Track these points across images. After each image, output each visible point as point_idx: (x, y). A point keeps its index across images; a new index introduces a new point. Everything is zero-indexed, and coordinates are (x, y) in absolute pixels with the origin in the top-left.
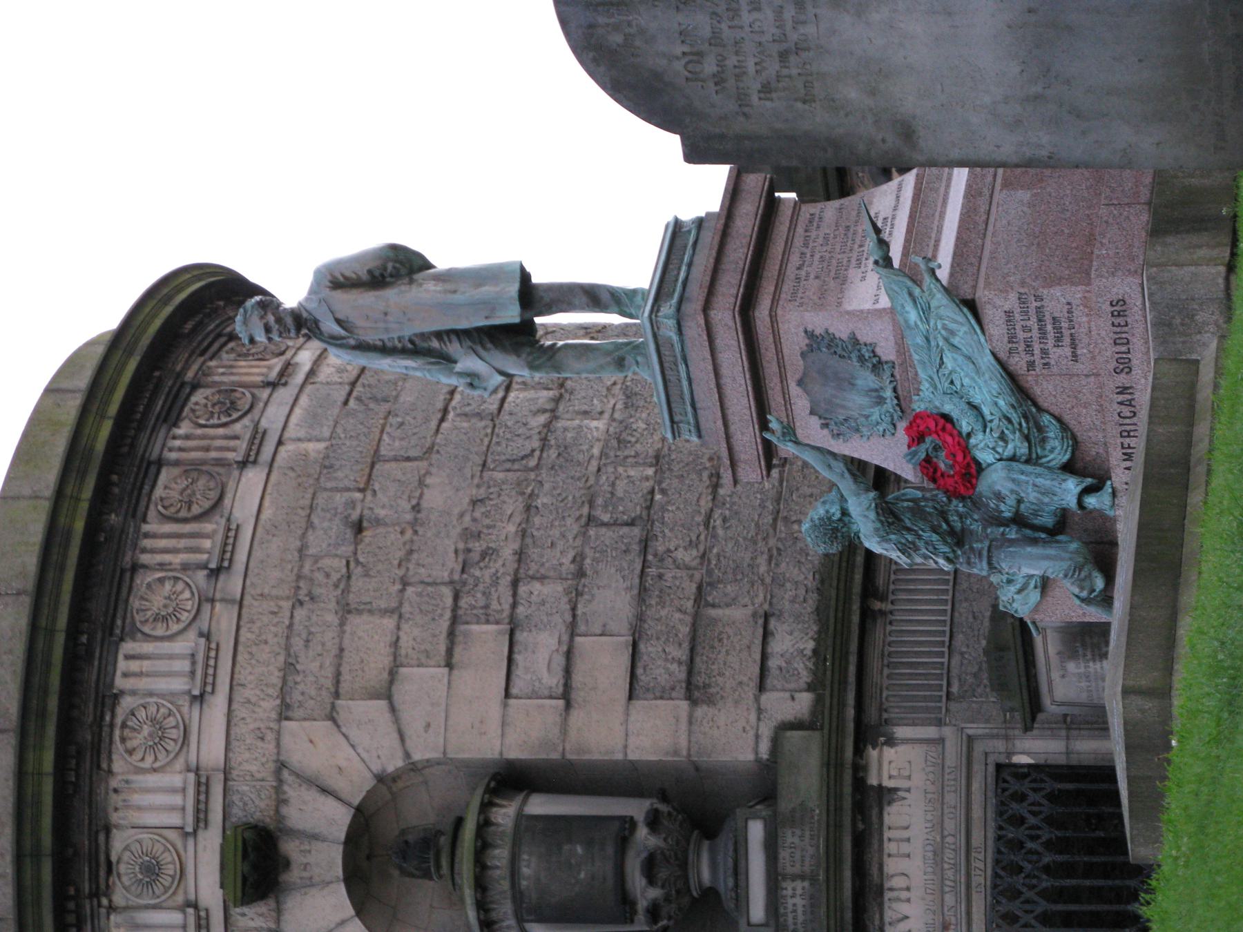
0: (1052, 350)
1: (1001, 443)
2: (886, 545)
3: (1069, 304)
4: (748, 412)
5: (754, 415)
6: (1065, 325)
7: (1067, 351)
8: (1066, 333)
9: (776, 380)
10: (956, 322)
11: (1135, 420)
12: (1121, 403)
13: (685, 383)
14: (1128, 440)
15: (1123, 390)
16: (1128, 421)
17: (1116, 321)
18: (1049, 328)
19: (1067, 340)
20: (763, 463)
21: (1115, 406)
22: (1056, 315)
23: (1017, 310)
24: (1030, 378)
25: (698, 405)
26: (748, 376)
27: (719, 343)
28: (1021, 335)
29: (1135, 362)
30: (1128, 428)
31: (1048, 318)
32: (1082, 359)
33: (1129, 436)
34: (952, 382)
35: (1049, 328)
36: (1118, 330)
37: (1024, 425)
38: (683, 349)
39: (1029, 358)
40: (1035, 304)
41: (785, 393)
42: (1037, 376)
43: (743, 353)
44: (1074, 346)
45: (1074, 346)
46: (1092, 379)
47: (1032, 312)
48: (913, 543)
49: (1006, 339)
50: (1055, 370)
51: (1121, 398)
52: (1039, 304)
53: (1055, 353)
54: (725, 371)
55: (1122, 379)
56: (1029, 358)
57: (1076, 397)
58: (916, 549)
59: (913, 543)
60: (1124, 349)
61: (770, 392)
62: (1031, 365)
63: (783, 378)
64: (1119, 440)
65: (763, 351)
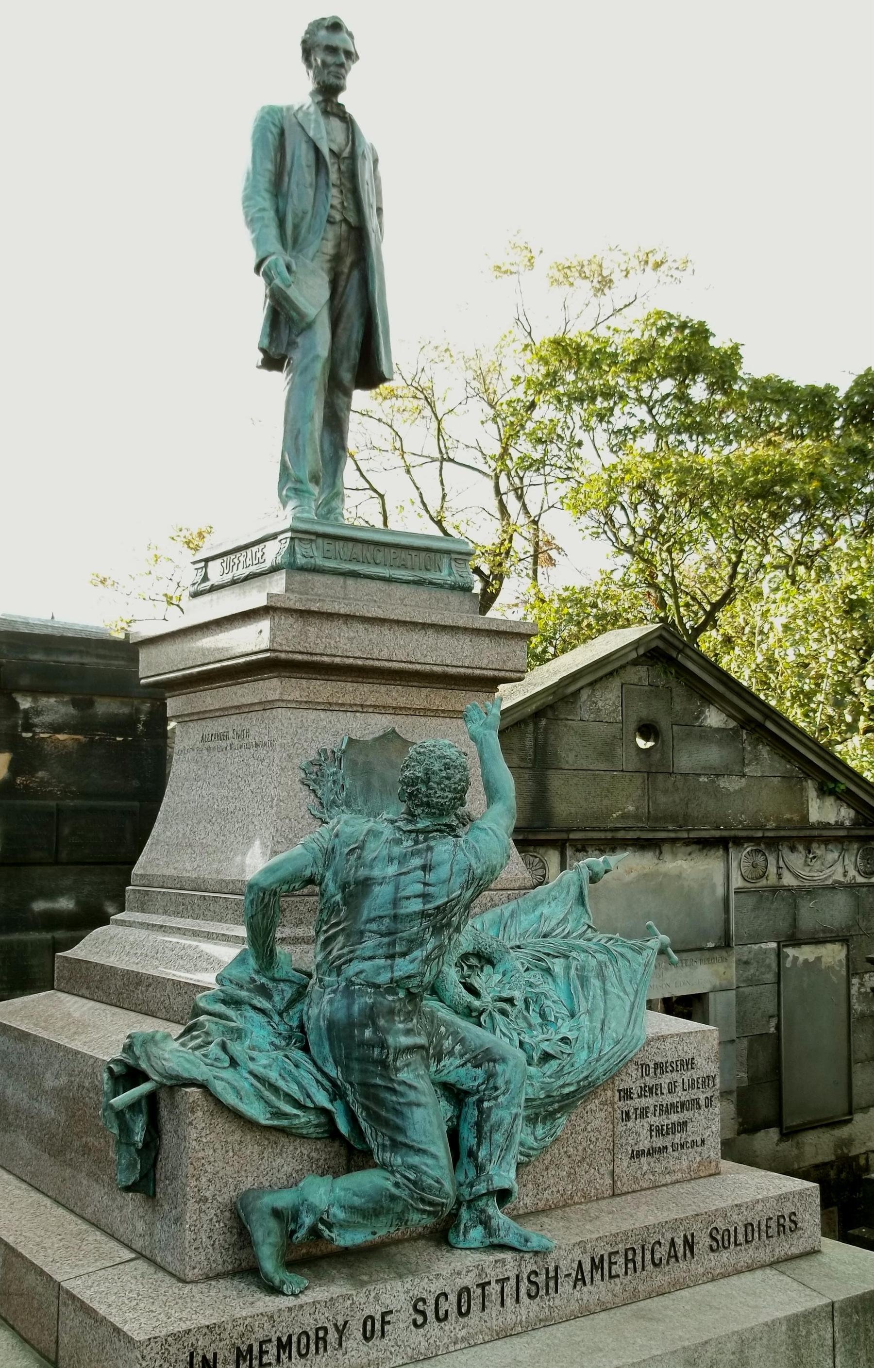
0: (645, 1123)
1: (536, 1058)
2: (458, 881)
3: (703, 1141)
4: (385, 654)
5: (377, 664)
6: (678, 1138)
7: (645, 1144)
8: (667, 1141)
9: (402, 702)
10: (620, 980)
11: (649, 1267)
12: (673, 1243)
13: (386, 572)
14: (622, 1260)
15: (689, 1244)
16: (648, 1256)
17: (773, 1224)
18: (674, 1118)
19: (659, 1142)
20: (300, 657)
21: (669, 1236)
22: (690, 1126)
23: (695, 1074)
24: (609, 1093)
25: (350, 582)
26: (435, 668)
27: (485, 642)
28: (665, 1080)
29: (725, 1254)
30: (639, 1259)
31: (686, 1115)
32: (635, 1165)
33: (627, 1261)
34: (527, 969)
35: (674, 1118)
36: (763, 1227)
37: (567, 1090)
38: (431, 583)
39: (636, 1091)
40: (702, 1097)
41: (380, 709)
42: (613, 1104)
43: (470, 671)
44: (651, 1152)
45: (651, 1152)
46: (608, 1181)
47: (694, 1094)
48: (449, 925)
49: (659, 1059)
50: (621, 1128)
51: (679, 1242)
52: (702, 1102)
53: (641, 1127)
54: (445, 639)
55: (703, 1241)
56: (636, 1091)
57: (584, 1159)
58: (437, 930)
59: (449, 925)
60: (741, 1238)
61: (383, 689)
62: (626, 1094)
63: (397, 710)
64: (621, 1247)
65: (443, 692)
